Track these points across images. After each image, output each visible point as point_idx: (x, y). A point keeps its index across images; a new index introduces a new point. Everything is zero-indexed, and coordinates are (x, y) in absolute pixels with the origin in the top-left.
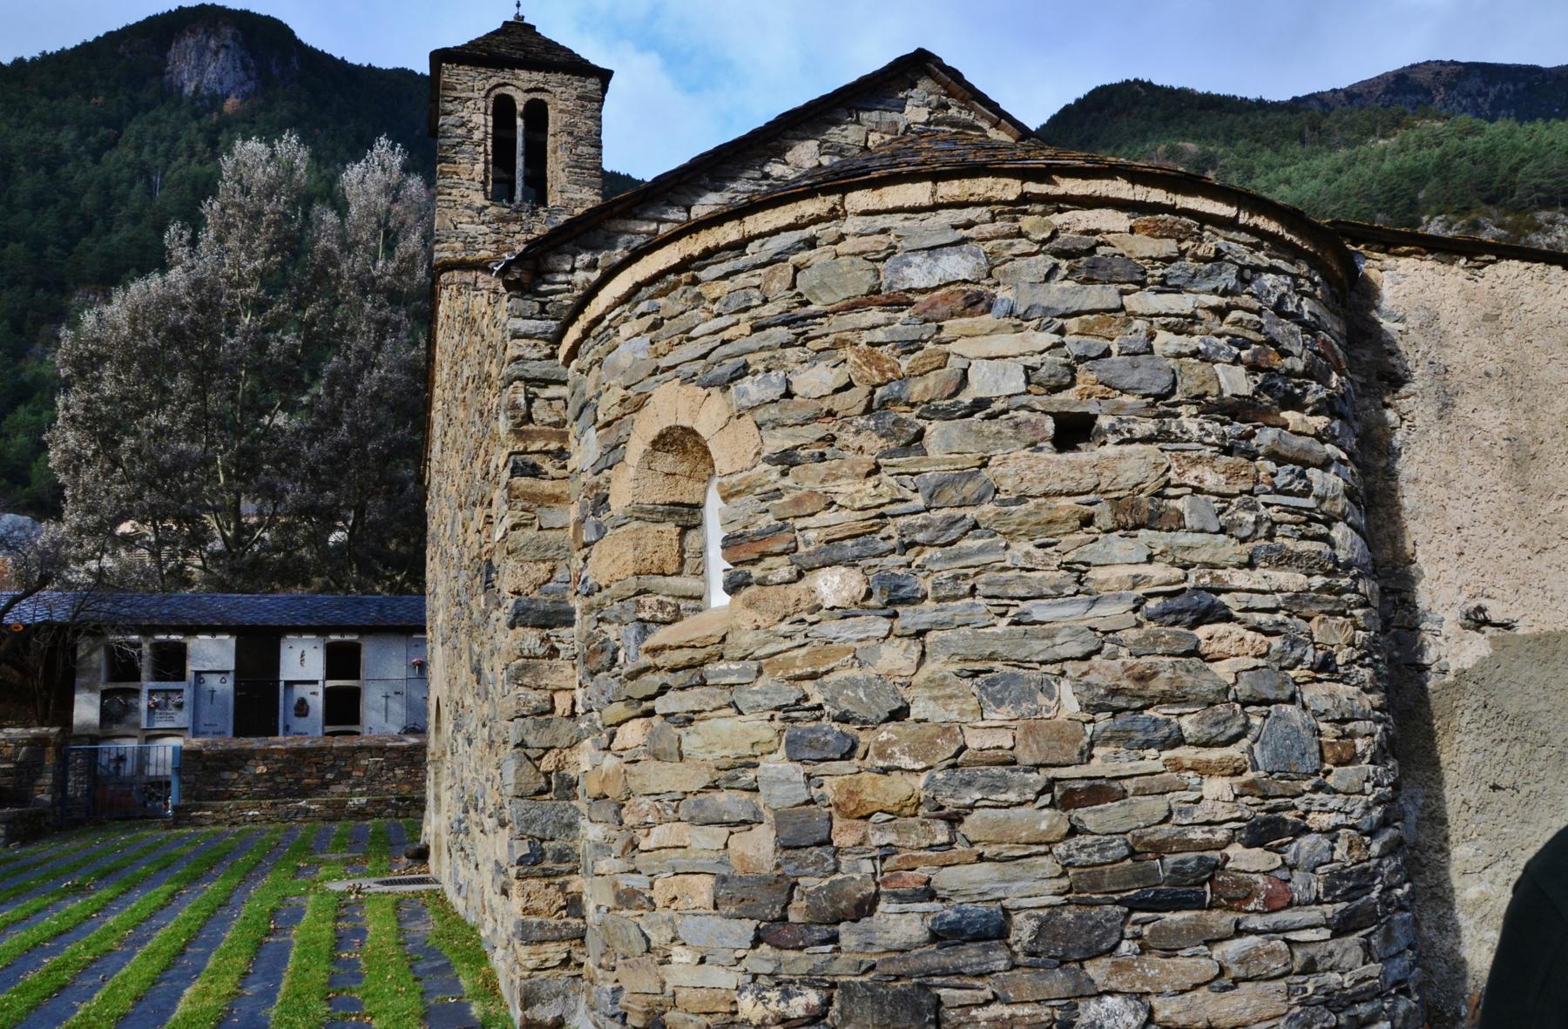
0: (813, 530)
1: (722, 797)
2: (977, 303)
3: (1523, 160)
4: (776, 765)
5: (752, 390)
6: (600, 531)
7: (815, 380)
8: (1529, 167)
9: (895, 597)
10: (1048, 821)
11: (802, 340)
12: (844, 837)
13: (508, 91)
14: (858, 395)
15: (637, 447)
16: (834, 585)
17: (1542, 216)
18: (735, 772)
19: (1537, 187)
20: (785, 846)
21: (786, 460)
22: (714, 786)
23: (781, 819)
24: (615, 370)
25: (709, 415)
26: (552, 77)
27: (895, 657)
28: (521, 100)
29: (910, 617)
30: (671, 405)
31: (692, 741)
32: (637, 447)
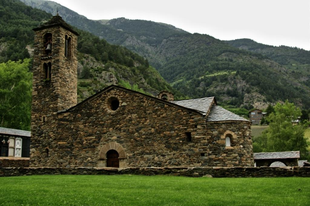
0: (241, 142)
1: (234, 159)
2: (247, 130)
3: (83, 41)
4: (238, 157)
5: (236, 133)
6: (219, 140)
7: (240, 133)
8: (85, 43)
9: (244, 147)
10: (250, 161)
11: (239, 130)
12: (243, 162)
13: (67, 35)
14: (242, 135)
15: (225, 134)
16: (242, 146)
17: (86, 55)
18: (235, 157)
19: (86, 48)
20: (239, 162)
21: (238, 138)
22: (234, 158)
23: (239, 160)
24: (221, 127)
25: (233, 134)
26: (73, 34)
27: (244, 151)
28: (68, 36)
29: (245, 149)
30: (228, 132)
31: (231, 155)
32: (225, 134)
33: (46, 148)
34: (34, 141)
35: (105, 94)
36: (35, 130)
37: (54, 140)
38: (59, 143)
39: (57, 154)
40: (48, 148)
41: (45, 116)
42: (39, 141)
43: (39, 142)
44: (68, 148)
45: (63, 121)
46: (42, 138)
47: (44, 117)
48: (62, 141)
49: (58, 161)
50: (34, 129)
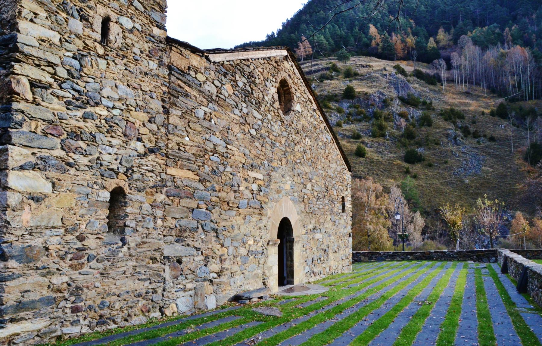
33: (112, 184)
34: (42, 126)
35: (276, 62)
36: (50, 64)
37: (152, 151)
38: (172, 171)
39: (164, 219)
40: (127, 190)
41: (114, 17)
42: (76, 135)
43: (74, 143)
44: (201, 199)
45: (185, 83)
46: (90, 126)
47: (106, 21)
48: (182, 167)
49: (168, 251)
50: (40, 54)
